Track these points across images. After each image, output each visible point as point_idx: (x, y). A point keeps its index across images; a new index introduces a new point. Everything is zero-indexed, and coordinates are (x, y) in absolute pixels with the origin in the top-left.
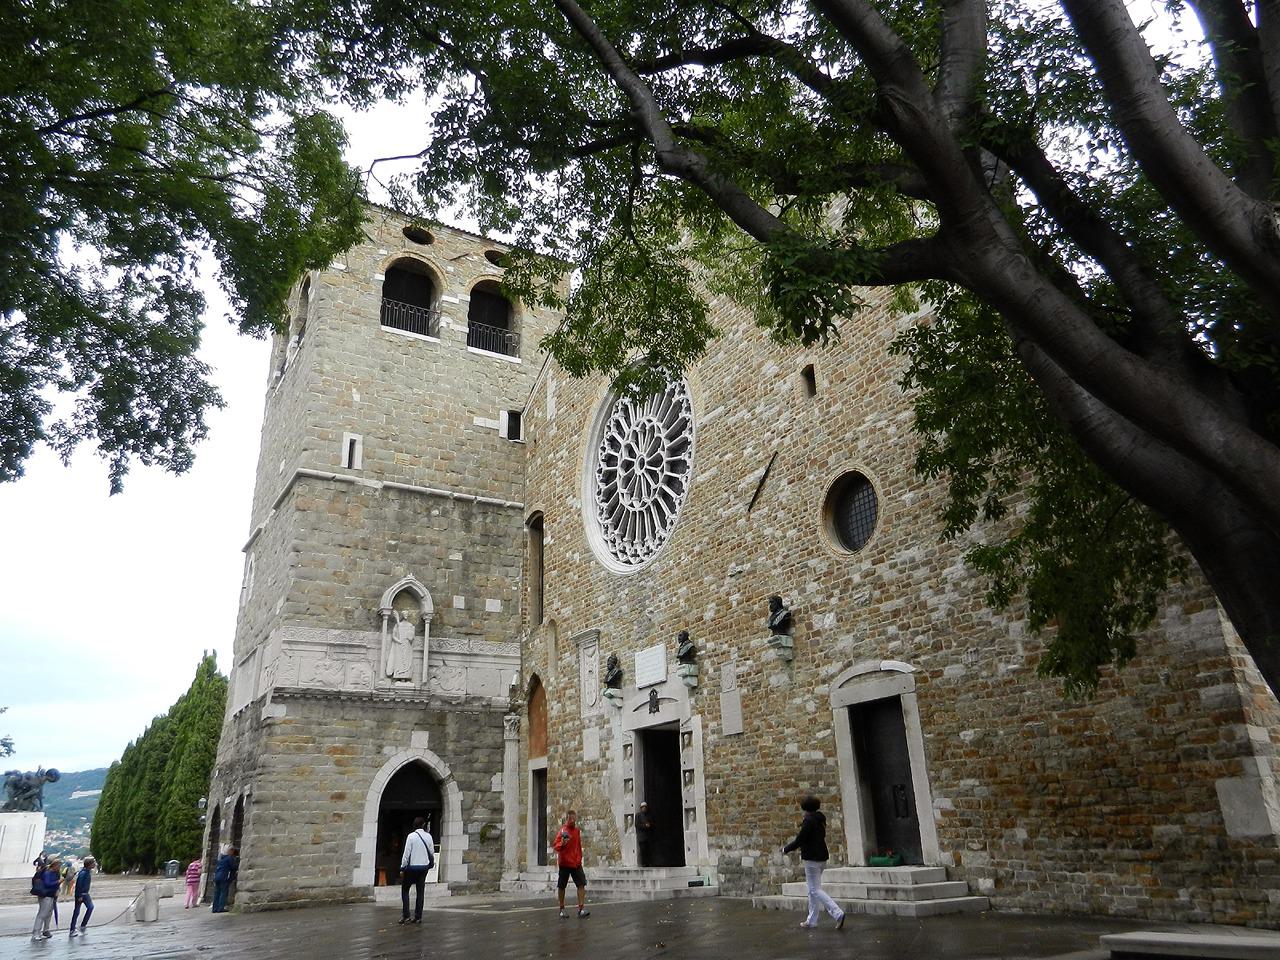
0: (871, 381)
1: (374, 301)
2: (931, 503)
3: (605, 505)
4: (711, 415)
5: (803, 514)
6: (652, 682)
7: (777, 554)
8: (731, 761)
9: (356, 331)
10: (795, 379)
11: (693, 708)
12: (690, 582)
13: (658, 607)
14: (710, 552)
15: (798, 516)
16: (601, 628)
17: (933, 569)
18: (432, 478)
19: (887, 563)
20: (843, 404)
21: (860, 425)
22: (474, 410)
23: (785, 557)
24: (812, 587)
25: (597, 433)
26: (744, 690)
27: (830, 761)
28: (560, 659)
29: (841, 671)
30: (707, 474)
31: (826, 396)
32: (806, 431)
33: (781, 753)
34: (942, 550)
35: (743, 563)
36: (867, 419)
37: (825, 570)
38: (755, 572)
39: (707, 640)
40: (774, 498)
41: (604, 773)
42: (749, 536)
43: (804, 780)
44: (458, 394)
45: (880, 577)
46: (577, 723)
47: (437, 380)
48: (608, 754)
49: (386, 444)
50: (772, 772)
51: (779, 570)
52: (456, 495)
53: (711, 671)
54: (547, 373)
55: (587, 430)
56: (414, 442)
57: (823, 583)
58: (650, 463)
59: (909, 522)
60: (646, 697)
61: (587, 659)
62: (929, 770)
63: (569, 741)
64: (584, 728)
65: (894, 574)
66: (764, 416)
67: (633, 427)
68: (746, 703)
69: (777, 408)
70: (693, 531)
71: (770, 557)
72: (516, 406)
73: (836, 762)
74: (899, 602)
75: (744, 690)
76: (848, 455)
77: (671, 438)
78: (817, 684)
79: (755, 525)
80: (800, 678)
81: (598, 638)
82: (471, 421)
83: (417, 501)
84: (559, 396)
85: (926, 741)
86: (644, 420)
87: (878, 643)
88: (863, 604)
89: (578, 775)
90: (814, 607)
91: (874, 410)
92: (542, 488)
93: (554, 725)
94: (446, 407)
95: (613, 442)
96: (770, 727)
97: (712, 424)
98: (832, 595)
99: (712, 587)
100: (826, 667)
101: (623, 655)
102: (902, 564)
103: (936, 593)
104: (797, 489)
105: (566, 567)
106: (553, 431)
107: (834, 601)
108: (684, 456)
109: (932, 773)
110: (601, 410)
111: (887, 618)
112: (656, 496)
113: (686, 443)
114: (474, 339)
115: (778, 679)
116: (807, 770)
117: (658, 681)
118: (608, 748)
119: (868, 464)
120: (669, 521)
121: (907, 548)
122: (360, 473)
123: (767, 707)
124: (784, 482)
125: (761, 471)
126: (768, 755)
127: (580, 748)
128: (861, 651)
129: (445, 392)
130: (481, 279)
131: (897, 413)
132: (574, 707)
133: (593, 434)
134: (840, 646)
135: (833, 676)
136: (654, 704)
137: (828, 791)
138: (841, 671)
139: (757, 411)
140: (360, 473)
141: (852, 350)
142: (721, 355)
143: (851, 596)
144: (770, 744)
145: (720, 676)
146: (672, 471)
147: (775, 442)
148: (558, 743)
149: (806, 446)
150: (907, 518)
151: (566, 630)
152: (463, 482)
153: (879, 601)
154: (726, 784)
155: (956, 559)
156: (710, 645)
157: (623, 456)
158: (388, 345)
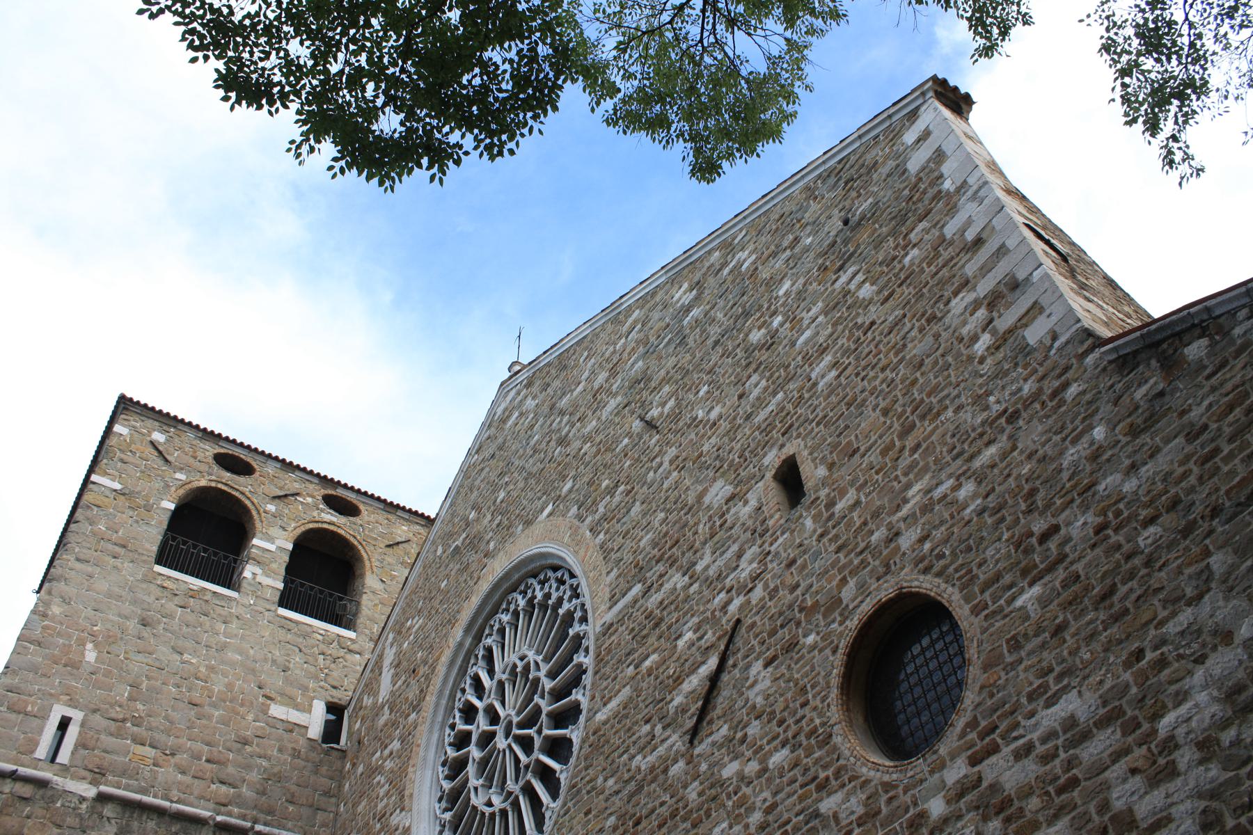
0: (907, 430)
1: (152, 534)
2: (1087, 589)
3: (448, 816)
7: (751, 810)
9: (115, 567)
10: (765, 492)
15: (791, 721)
17: (1131, 726)
18: (185, 789)
19: (1007, 750)
20: (858, 490)
21: (898, 508)
22: (273, 695)
23: (768, 811)
25: (444, 702)
30: (613, 704)
31: (823, 493)
32: (793, 562)
34: (1142, 677)
36: (911, 493)
37: (860, 810)
40: (740, 703)
42: (692, 793)
44: (253, 671)
47: (222, 648)
49: (119, 729)
52: (219, 818)
55: (430, 699)
56: (168, 732)
58: (521, 726)
59: (1043, 646)
65: (1030, 769)
66: (711, 572)
67: (499, 675)
69: (735, 548)
70: (586, 814)
72: (340, 696)
76: (881, 570)
77: (552, 675)
79: (704, 767)
82: (265, 711)
83: (151, 825)
84: (398, 666)
86: (514, 658)
91: (926, 469)
92: (360, 808)
94: (230, 686)
95: (469, 713)
102: (1044, 740)
103: (1154, 782)
104: (783, 669)
106: (386, 716)
108: (577, 695)
112: (529, 776)
113: (581, 670)
114: (287, 599)
119: (926, 571)
120: (548, 815)
121: (1050, 704)
122: (65, 769)
124: (757, 666)
125: (713, 662)
129: (233, 664)
130: (311, 526)
131: (972, 458)
133: (437, 705)
139: (699, 568)
140: (65, 769)
141: (864, 400)
142: (637, 508)
146: (556, 728)
147: (737, 603)
149: (795, 587)
150: (1040, 639)
152: (238, 801)
155: (1186, 684)
157: (482, 724)
158: (158, 592)
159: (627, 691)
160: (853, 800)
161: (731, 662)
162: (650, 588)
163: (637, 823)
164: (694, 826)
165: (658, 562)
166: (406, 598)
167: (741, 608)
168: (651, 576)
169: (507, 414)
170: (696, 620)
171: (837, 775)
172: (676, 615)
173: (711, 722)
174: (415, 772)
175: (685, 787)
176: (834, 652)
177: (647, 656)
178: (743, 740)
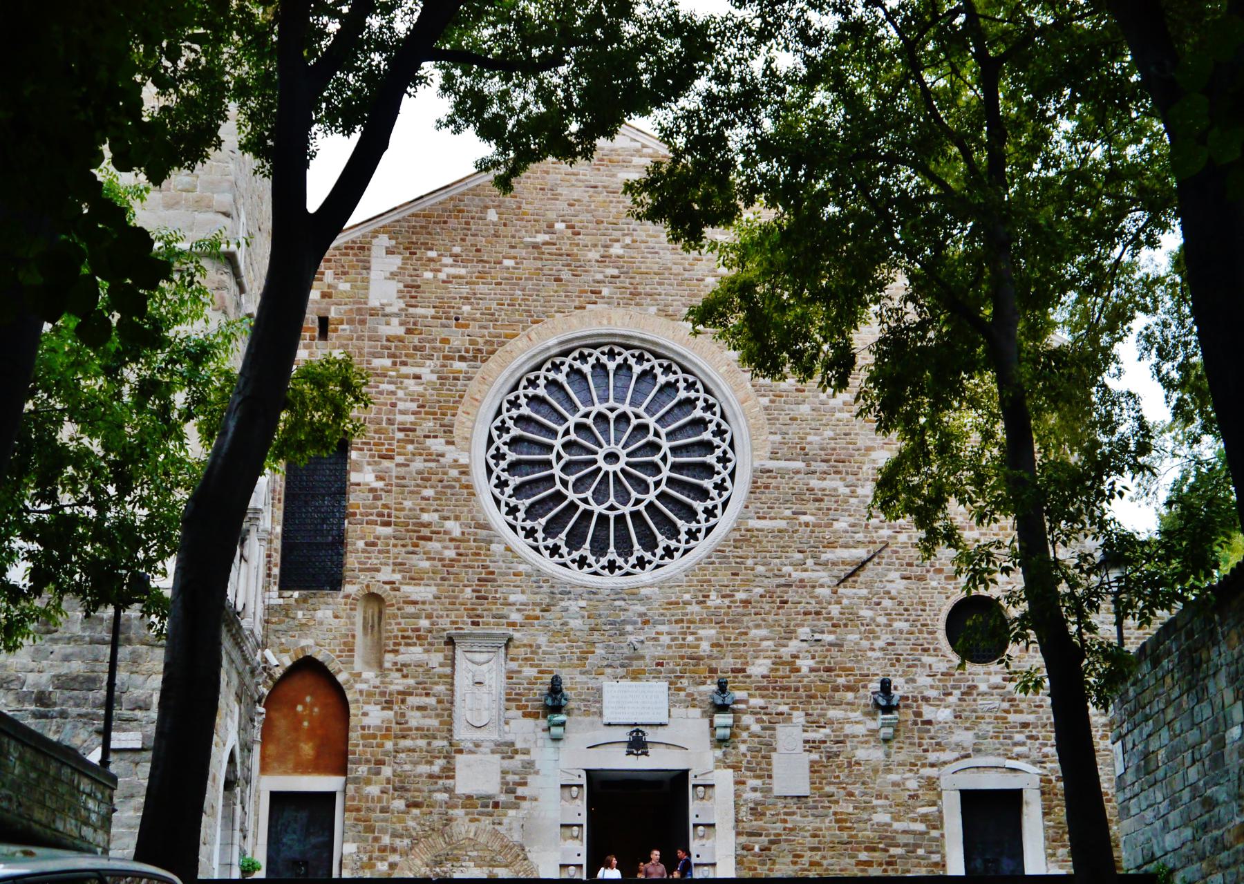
4: (782, 464)
5: (920, 613)
6: (639, 721)
7: (878, 638)
8: (785, 821)
11: (718, 760)
12: (724, 627)
13: (656, 639)
14: (767, 607)
16: (516, 635)
23: (889, 644)
24: (923, 680)
25: (512, 381)
26: (815, 756)
27: (935, 833)
28: (395, 652)
29: (957, 759)
33: (866, 821)
35: (823, 632)
37: (944, 670)
38: (842, 646)
39: (750, 695)
41: (512, 813)
43: (897, 846)
45: (1009, 692)
46: (439, 743)
48: (520, 791)
50: (851, 836)
51: (879, 654)
53: (756, 728)
54: (375, 233)
57: (940, 680)
60: (623, 734)
61: (470, 665)
62: (1046, 848)
63: (415, 764)
64: (460, 751)
68: (814, 768)
70: (733, 574)
71: (867, 638)
73: (942, 835)
74: (1030, 718)
75: (815, 756)
78: (923, 765)
80: (901, 757)
81: (507, 646)
85: (1046, 828)
87: (1002, 744)
88: (990, 710)
89: (436, 810)
90: (926, 699)
93: (374, 737)
96: (851, 794)
97: (782, 473)
98: (950, 694)
99: (765, 644)
100: (938, 754)
101: (572, 681)
105: (420, 534)
107: (951, 699)
109: (1050, 851)
110: (534, 356)
111: (1015, 727)
115: (872, 754)
116: (902, 839)
117: (658, 721)
118: (525, 784)
123: (847, 777)
125: (861, 553)
126: (845, 821)
127: (449, 772)
128: (983, 747)
132: (434, 723)
133: (506, 380)
134: (955, 738)
135: (945, 763)
136: (637, 744)
137: (928, 858)
138: (957, 759)
142: (805, 409)
143: (975, 700)
144: (851, 810)
145: (771, 736)
148: (382, 763)
151: (417, 617)
153: (1007, 711)
154: (772, 842)
156: (757, 702)
159: (782, 524)
160: (941, 664)
161: (876, 560)
162: (813, 473)
163: (786, 602)
164: (834, 626)
165: (823, 461)
166: (413, 215)
167: (889, 537)
168: (816, 466)
169: (615, 158)
170: (852, 520)
171: (935, 650)
172: (834, 506)
173: (855, 582)
174: (474, 422)
175: (830, 603)
176: (948, 598)
177: (805, 513)
178: (878, 604)
